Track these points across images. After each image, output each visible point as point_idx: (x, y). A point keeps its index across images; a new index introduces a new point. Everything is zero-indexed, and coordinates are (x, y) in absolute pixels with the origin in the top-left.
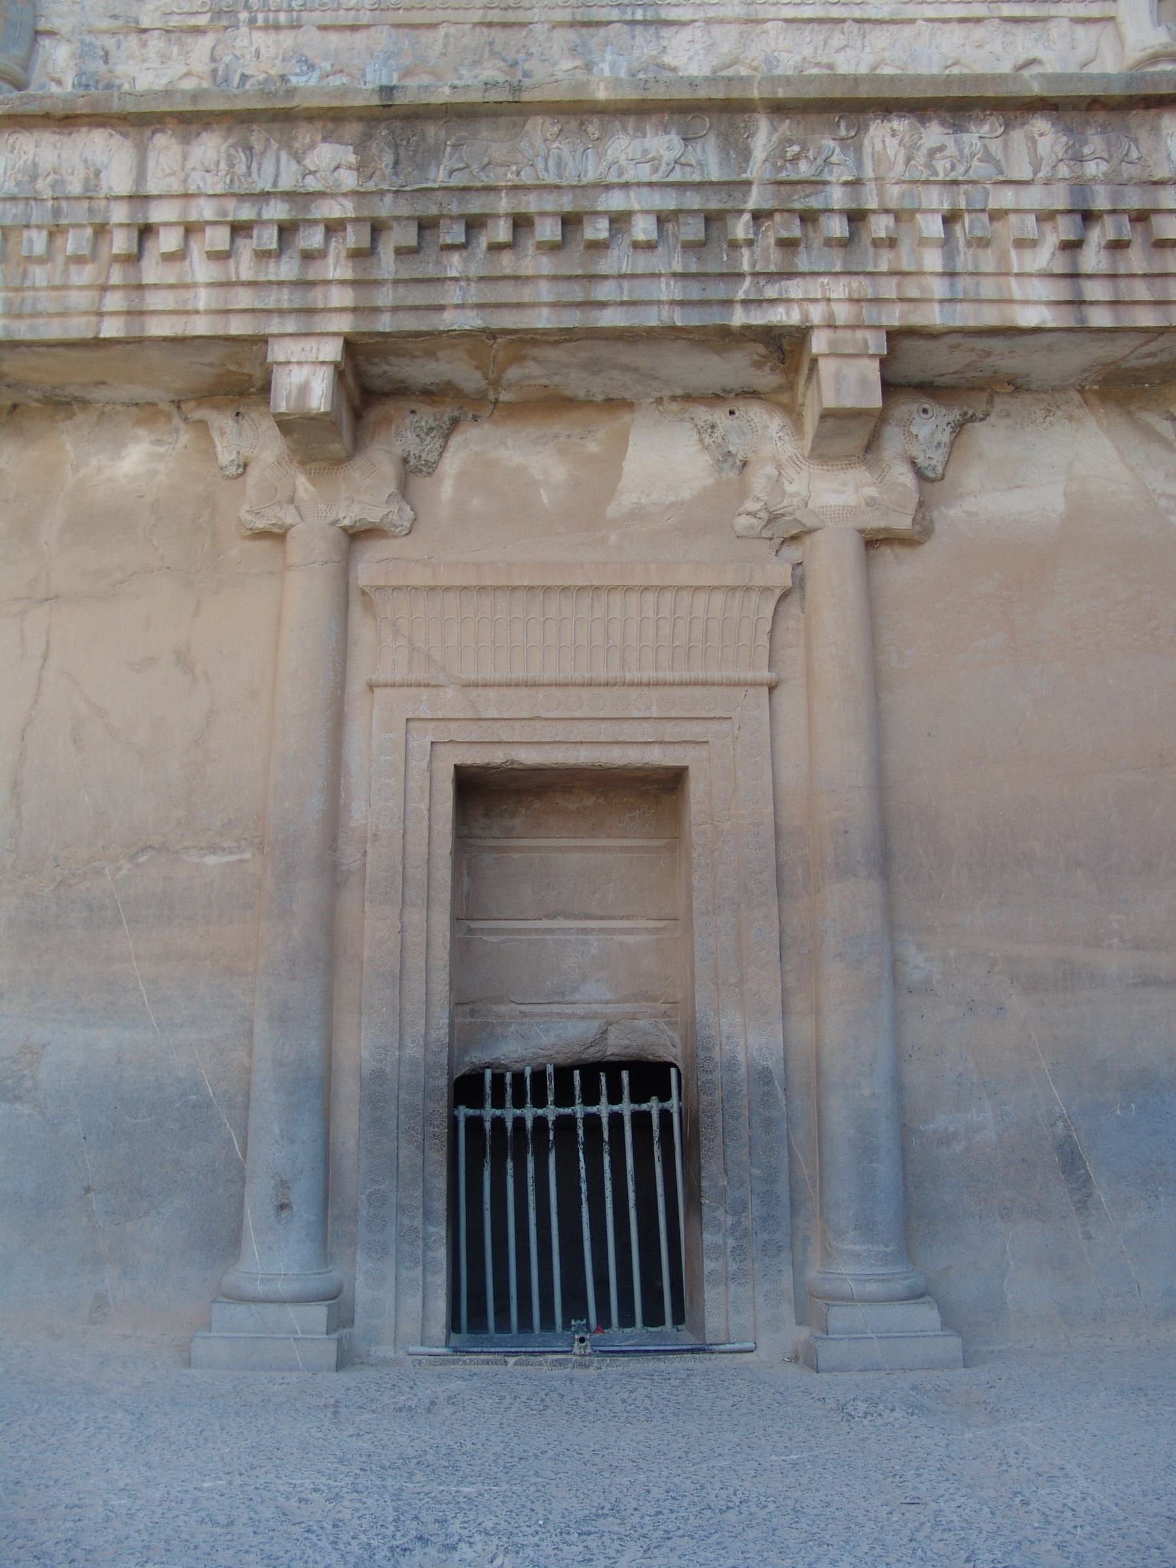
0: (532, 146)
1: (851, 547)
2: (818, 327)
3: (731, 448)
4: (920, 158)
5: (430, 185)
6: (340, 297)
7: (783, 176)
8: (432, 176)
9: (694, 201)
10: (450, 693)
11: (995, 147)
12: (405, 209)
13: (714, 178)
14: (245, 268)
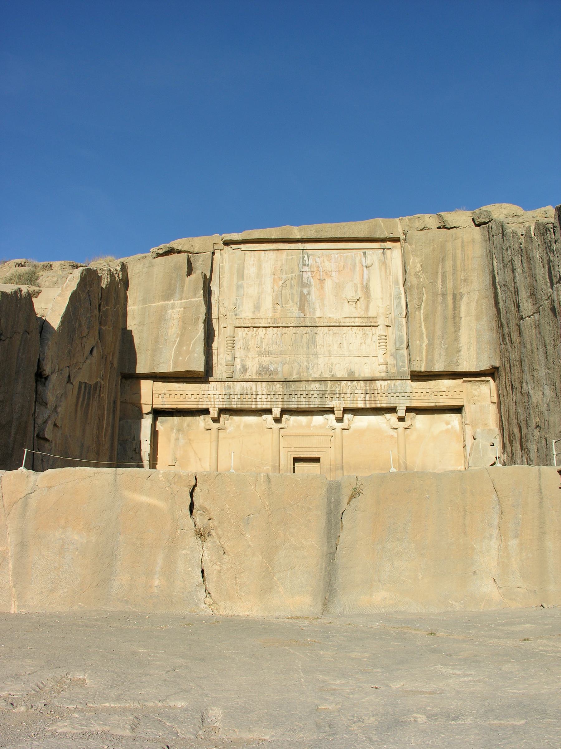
1: (340, 430)
4: (347, 387)
6: (280, 403)
10: (292, 448)
14: (269, 399)
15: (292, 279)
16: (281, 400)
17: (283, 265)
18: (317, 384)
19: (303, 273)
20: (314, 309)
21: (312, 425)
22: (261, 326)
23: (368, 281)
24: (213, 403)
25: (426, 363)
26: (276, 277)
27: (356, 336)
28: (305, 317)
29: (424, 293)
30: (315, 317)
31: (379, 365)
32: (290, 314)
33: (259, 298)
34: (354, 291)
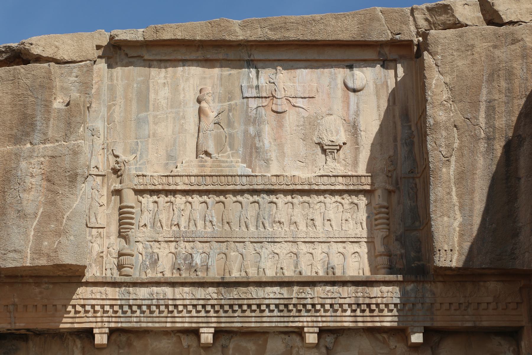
6: (214, 320)
7: (299, 297)
8: (231, 295)
9: (282, 302)
13: (286, 297)
15: (230, 110)
17: (215, 86)
18: (276, 289)
20: (267, 161)
22: (179, 188)
23: (357, 114)
26: (204, 104)
27: (338, 206)
30: (270, 175)
33: (175, 140)
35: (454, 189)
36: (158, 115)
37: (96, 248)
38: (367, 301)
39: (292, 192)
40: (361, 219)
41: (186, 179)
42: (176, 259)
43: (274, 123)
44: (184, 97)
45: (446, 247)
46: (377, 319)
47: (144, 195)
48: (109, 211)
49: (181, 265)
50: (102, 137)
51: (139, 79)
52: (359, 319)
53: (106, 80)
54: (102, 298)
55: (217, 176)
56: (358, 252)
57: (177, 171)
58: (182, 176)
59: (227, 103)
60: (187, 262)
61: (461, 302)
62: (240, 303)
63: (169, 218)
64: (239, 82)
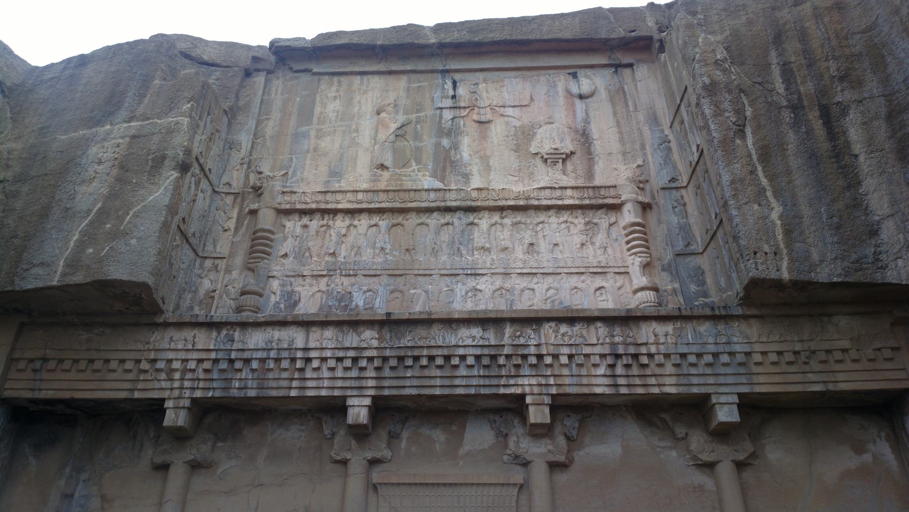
0: (435, 332)
2: (528, 394)
3: (501, 429)
5: (401, 345)
6: (371, 383)
7: (515, 343)
8: (402, 342)
9: (486, 351)
11: (584, 332)
12: (394, 353)
13: (493, 344)
15: (418, 122)
16: (373, 374)
17: (400, 99)
18: (476, 331)
19: (442, 112)
20: (467, 177)
21: (461, 452)
22: (340, 206)
23: (587, 121)
24: (176, 384)
25: (792, 260)
26: (383, 115)
27: (568, 228)
28: (444, 188)
29: (746, 102)
31: (636, 292)
32: (410, 183)
33: (342, 156)
34: (557, 140)
35: (760, 168)
36: (323, 129)
37: (206, 284)
38: (632, 350)
39: (501, 209)
40: (605, 243)
41: (350, 196)
42: (327, 299)
43: (476, 134)
44: (359, 110)
45: (766, 248)
46: (653, 381)
47: (291, 217)
48: (236, 239)
49: (333, 307)
50: (243, 152)
51: (303, 93)
52: (621, 381)
53: (260, 93)
54: (186, 348)
55: (394, 191)
56: (606, 286)
57: (340, 186)
58: (346, 192)
59: (413, 117)
60: (343, 304)
61: (796, 349)
62: (416, 354)
63: (323, 246)
64: (431, 94)
